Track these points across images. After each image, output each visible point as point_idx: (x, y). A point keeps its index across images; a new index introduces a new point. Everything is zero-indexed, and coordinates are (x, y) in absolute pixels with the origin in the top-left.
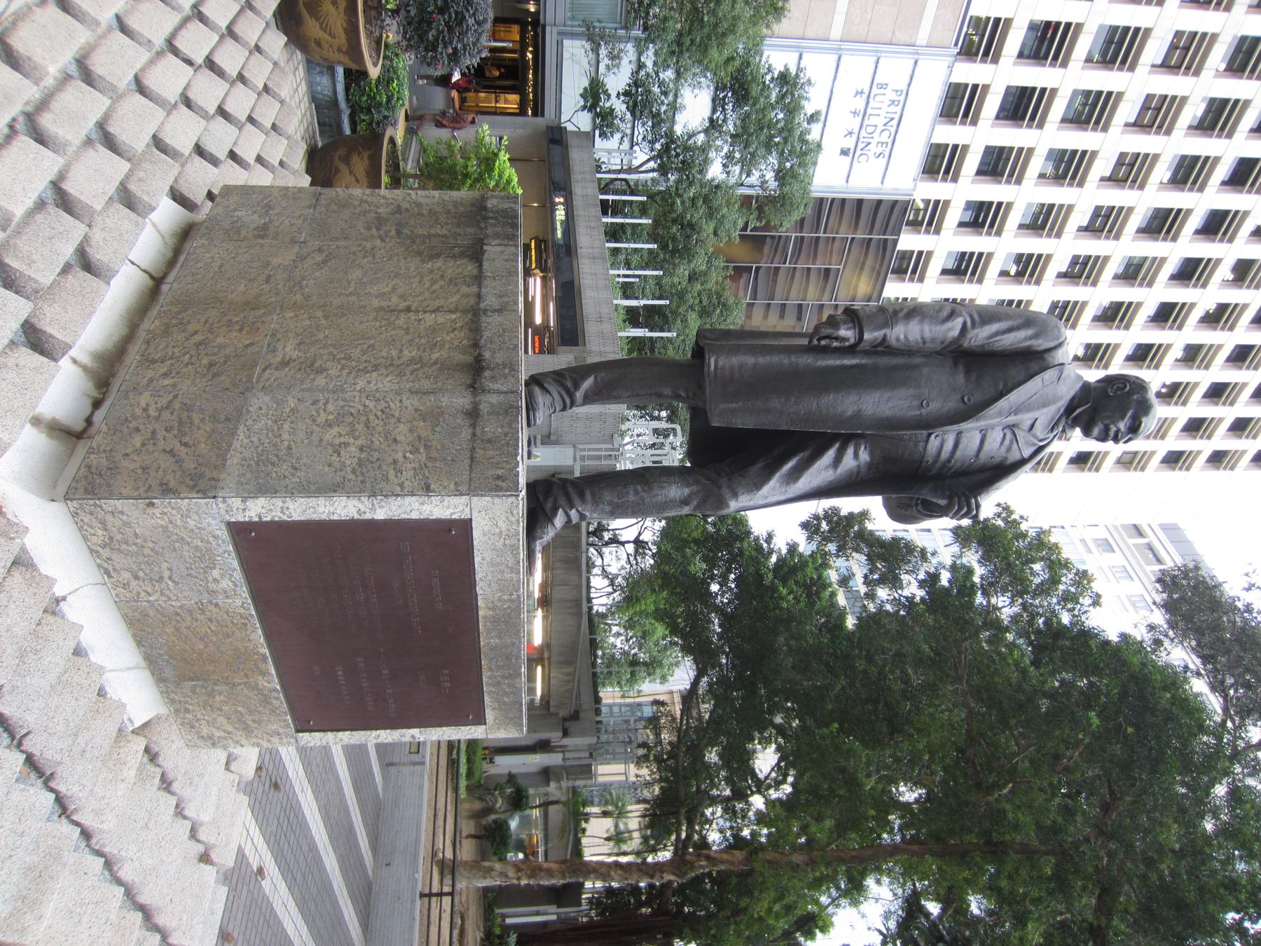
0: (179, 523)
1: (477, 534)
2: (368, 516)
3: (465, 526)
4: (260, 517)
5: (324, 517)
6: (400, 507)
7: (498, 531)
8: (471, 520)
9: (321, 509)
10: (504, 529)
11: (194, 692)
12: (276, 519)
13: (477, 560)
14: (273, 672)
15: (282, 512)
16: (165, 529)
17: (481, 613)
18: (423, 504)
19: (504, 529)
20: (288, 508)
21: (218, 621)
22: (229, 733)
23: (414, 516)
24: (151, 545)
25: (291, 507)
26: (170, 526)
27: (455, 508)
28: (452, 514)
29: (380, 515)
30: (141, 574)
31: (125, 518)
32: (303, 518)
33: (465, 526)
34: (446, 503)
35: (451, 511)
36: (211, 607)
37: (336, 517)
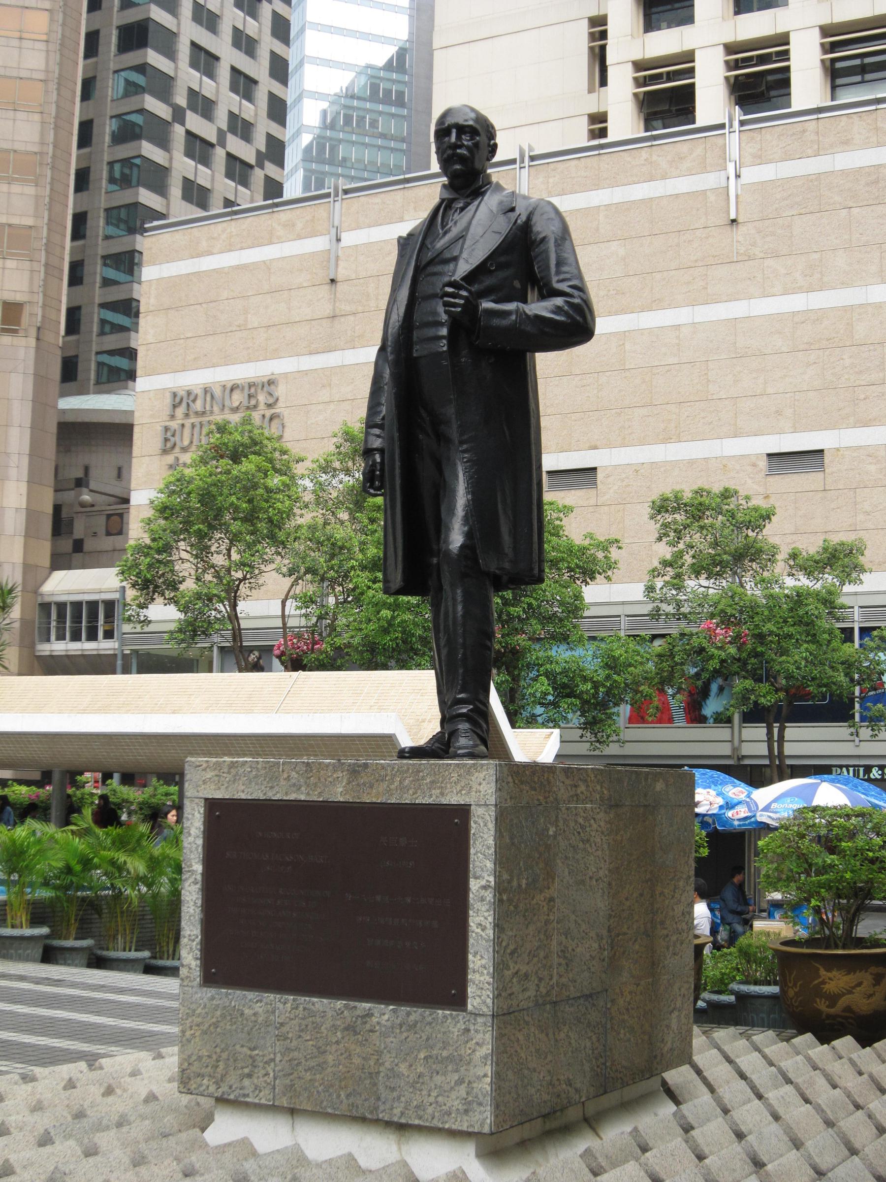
0: (199, 1020)
1: (219, 795)
2: (199, 877)
3: (213, 806)
4: (197, 959)
5: (198, 910)
6: (191, 852)
7: (216, 778)
8: (206, 799)
9: (192, 911)
10: (213, 773)
11: (393, 1089)
12: (199, 947)
13: (243, 796)
14: (367, 1005)
15: (193, 941)
16: (205, 1033)
17: (303, 797)
18: (190, 835)
19: (213, 773)
20: (190, 936)
21: (302, 1031)
22: (460, 1082)
23: (200, 842)
24: (218, 1050)
25: (189, 933)
26: (202, 1027)
27: (194, 809)
28: (199, 812)
29: (198, 868)
30: (246, 1071)
31: (194, 1058)
32: (199, 927)
33: (213, 806)
34: (190, 816)
35: (196, 814)
36: (284, 1029)
37: (199, 902)
